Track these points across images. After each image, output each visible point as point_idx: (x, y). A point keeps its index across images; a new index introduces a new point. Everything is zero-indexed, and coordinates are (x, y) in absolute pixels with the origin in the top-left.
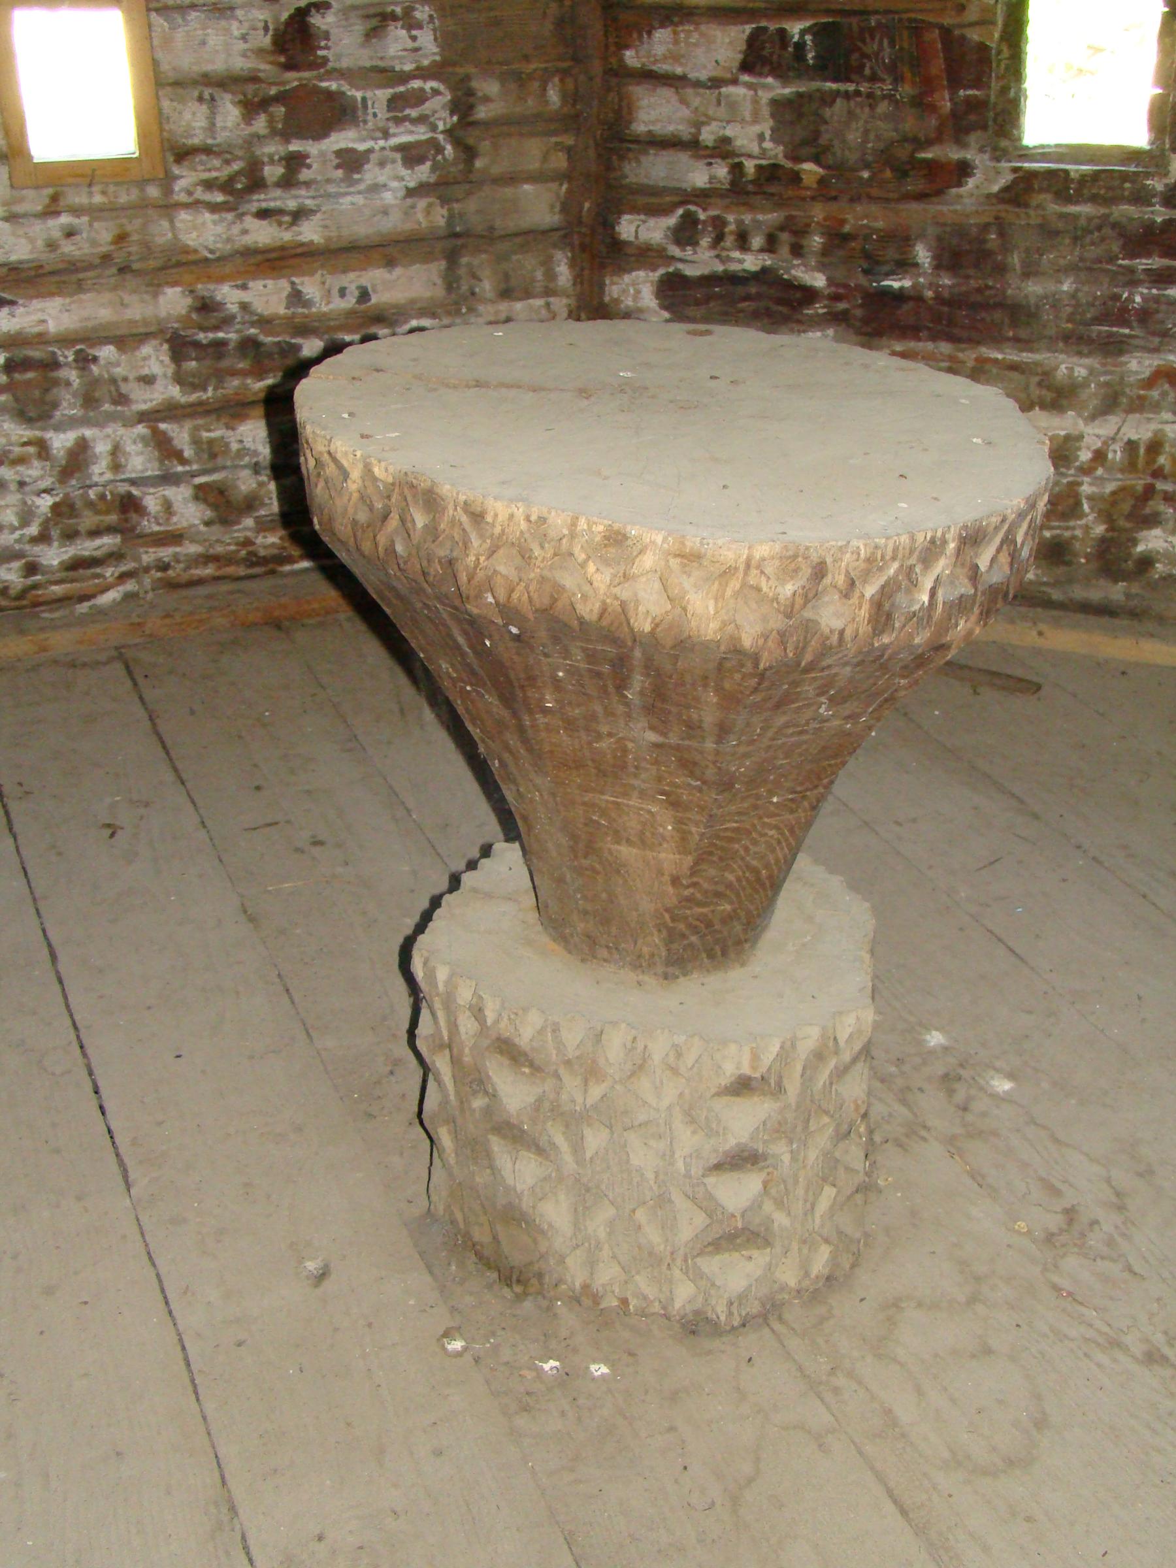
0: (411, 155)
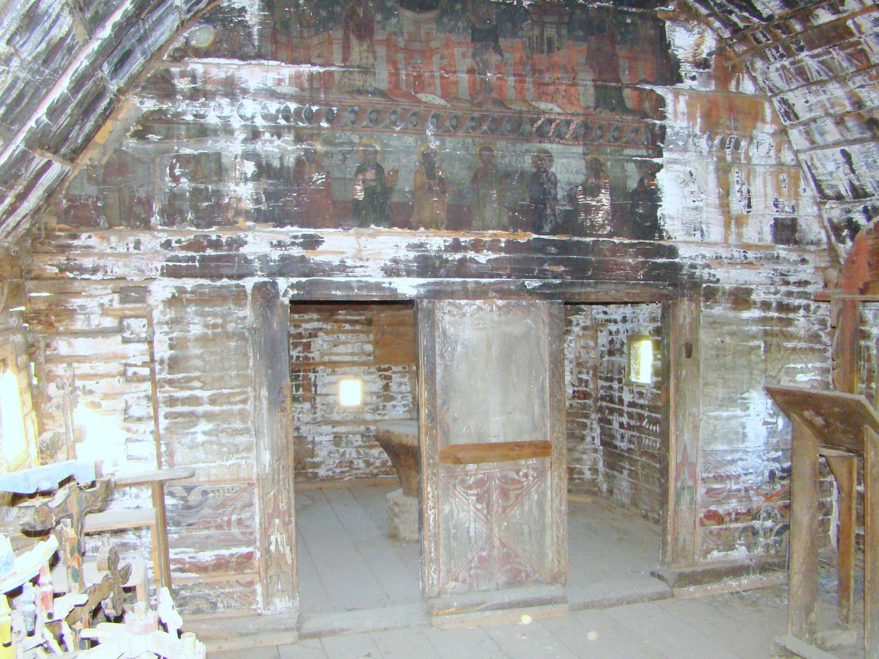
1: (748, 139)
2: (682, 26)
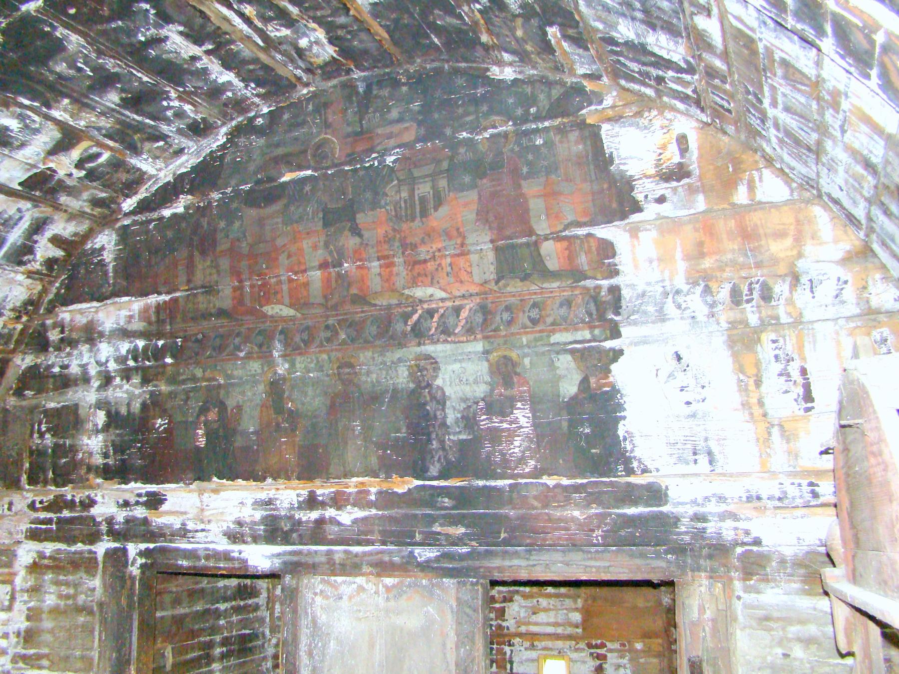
1: (788, 279)
2: (631, 125)
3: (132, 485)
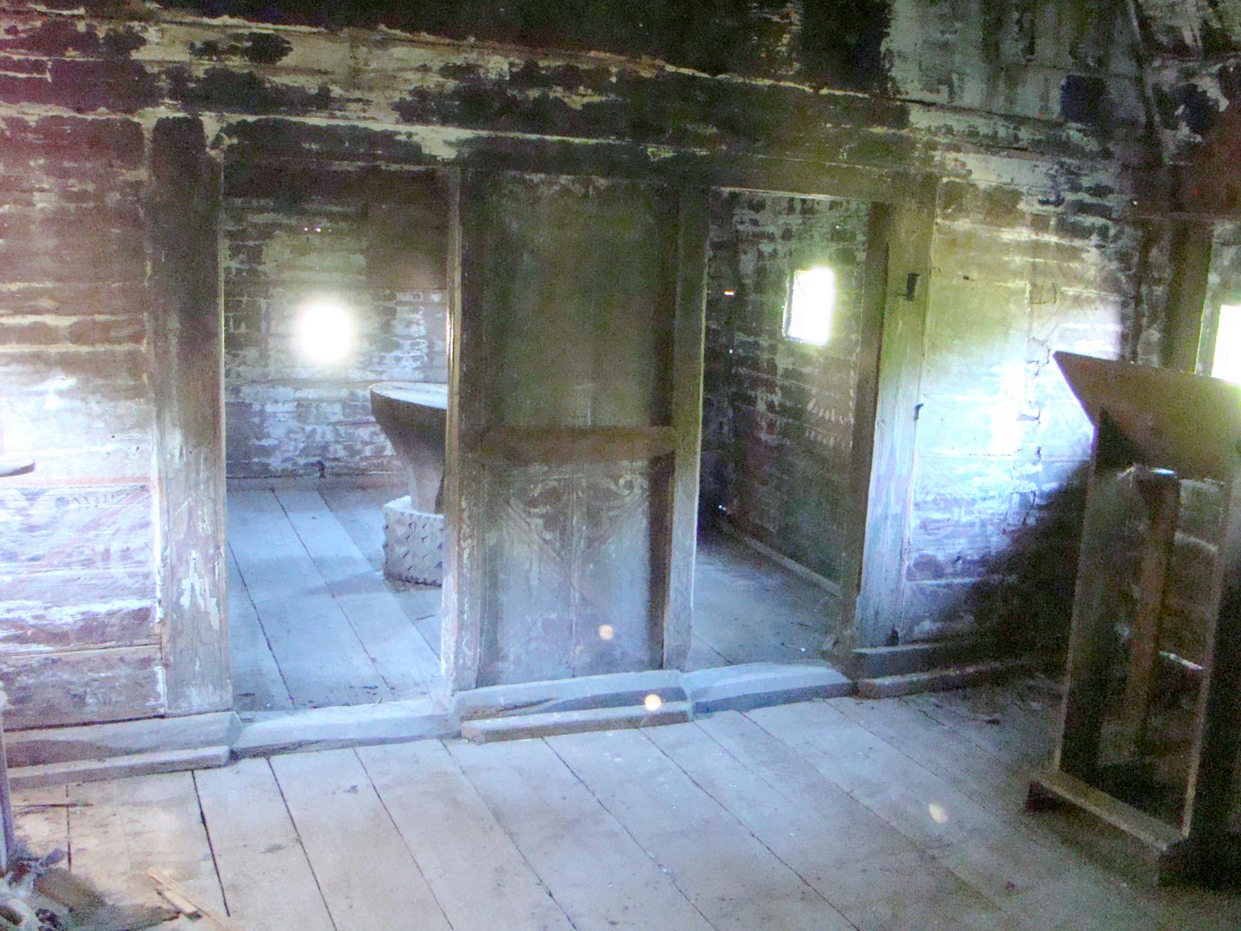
0: (415, 359)
3: (226, 19)
